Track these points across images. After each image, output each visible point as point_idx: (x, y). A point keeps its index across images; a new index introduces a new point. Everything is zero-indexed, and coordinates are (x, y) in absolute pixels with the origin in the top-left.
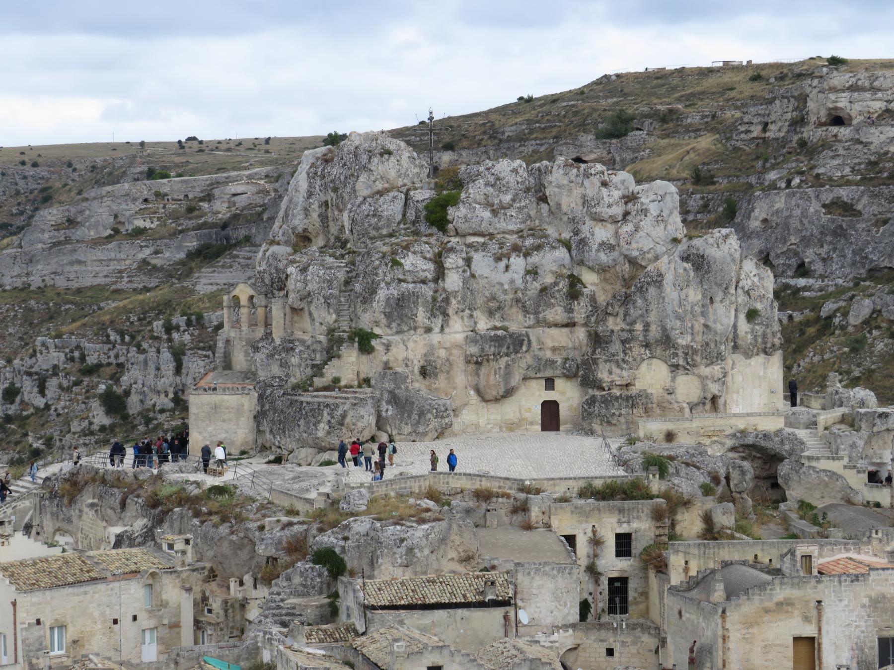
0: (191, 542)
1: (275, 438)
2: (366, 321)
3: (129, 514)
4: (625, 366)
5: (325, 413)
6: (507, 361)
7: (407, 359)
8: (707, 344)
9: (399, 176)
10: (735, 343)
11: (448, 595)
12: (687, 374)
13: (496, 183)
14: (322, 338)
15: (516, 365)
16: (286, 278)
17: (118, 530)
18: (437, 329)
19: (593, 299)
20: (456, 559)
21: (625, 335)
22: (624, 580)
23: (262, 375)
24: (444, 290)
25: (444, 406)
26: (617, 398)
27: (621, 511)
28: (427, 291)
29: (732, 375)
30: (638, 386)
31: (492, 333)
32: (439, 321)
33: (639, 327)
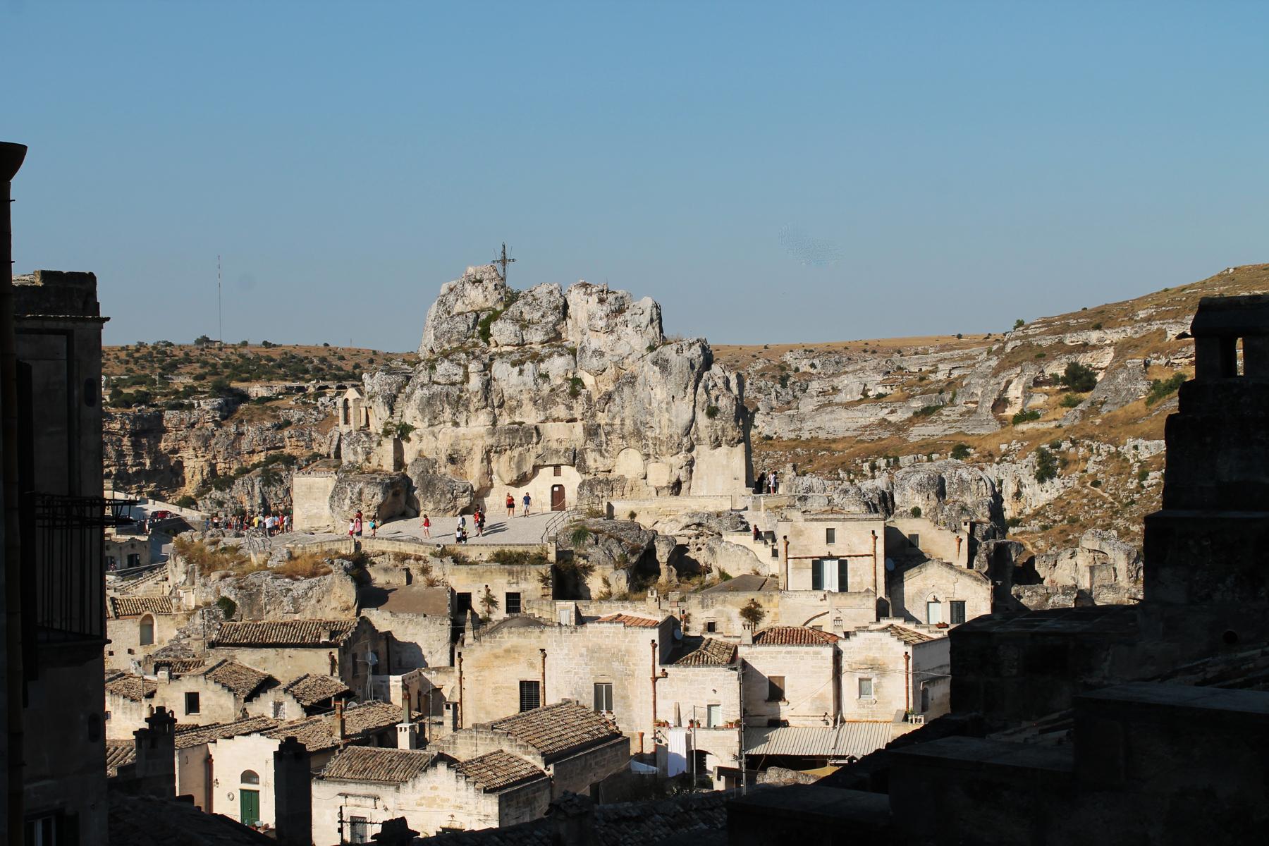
19: (589, 398)
21: (608, 428)
26: (600, 482)
27: (510, 573)
28: (455, 391)
33: (618, 421)
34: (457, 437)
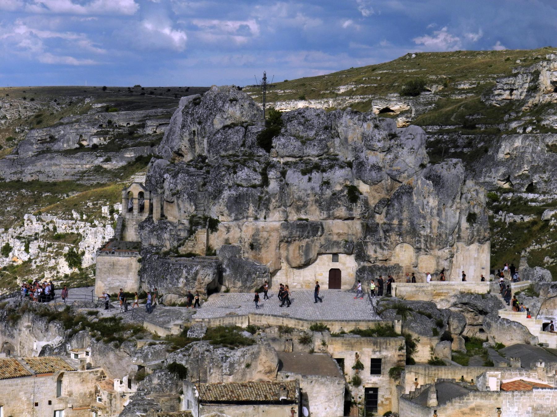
0: (90, 354)
1: (151, 287)
2: (214, 212)
3: (50, 334)
4: (385, 247)
5: (184, 271)
6: (307, 242)
7: (241, 237)
8: (440, 235)
9: (243, 116)
10: (459, 235)
11: (255, 395)
12: (426, 254)
13: (305, 123)
14: (186, 222)
15: (313, 244)
16: (164, 181)
17: (44, 343)
18: (262, 219)
19: (366, 203)
20: (263, 371)
21: (386, 227)
22: (376, 390)
23: (145, 244)
24: (267, 192)
25: (264, 270)
26: (379, 269)
27: (375, 344)
28: (257, 193)
29: (457, 256)
30: (393, 261)
31: (299, 223)
32: (263, 213)
33: (396, 222)
34: (257, 230)
